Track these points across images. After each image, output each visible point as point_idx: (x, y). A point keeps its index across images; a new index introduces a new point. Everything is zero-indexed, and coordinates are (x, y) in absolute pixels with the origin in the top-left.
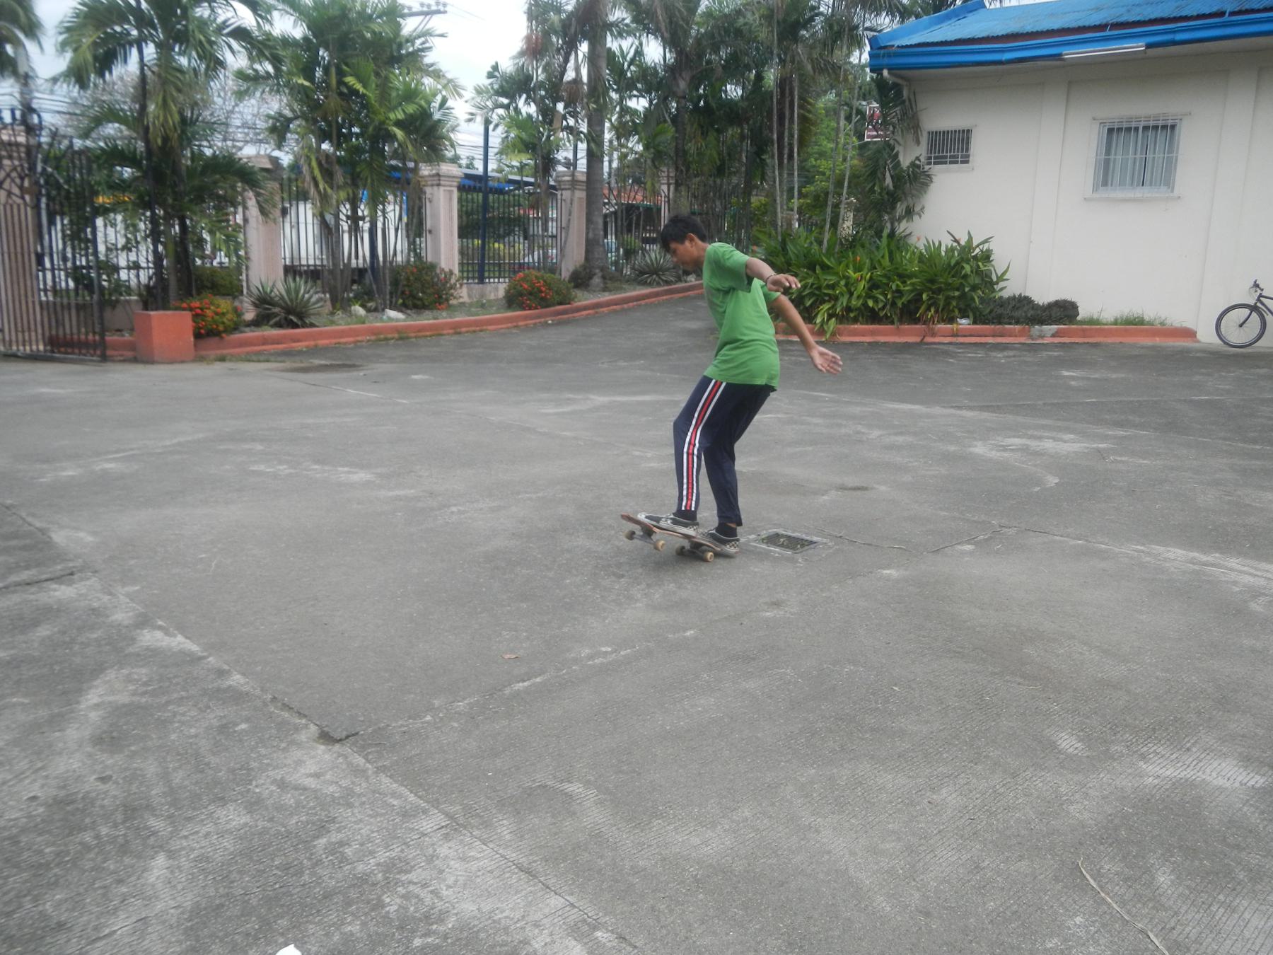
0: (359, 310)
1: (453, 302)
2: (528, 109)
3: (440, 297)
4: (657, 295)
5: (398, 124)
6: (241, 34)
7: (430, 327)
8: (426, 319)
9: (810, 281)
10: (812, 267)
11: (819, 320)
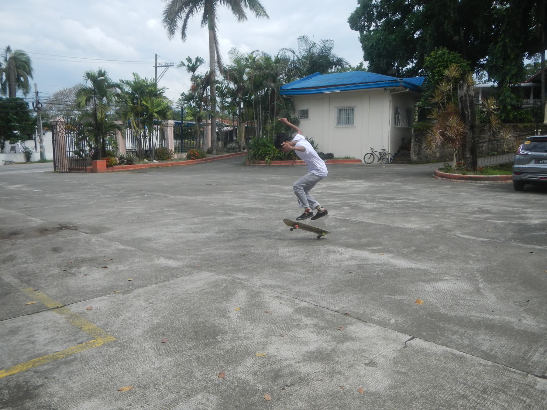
0: (147, 161)
1: (173, 158)
2: (193, 104)
4: (232, 155)
5: (156, 112)
6: (118, 95)
7: (165, 164)
8: (164, 163)
9: (264, 150)
10: (264, 146)
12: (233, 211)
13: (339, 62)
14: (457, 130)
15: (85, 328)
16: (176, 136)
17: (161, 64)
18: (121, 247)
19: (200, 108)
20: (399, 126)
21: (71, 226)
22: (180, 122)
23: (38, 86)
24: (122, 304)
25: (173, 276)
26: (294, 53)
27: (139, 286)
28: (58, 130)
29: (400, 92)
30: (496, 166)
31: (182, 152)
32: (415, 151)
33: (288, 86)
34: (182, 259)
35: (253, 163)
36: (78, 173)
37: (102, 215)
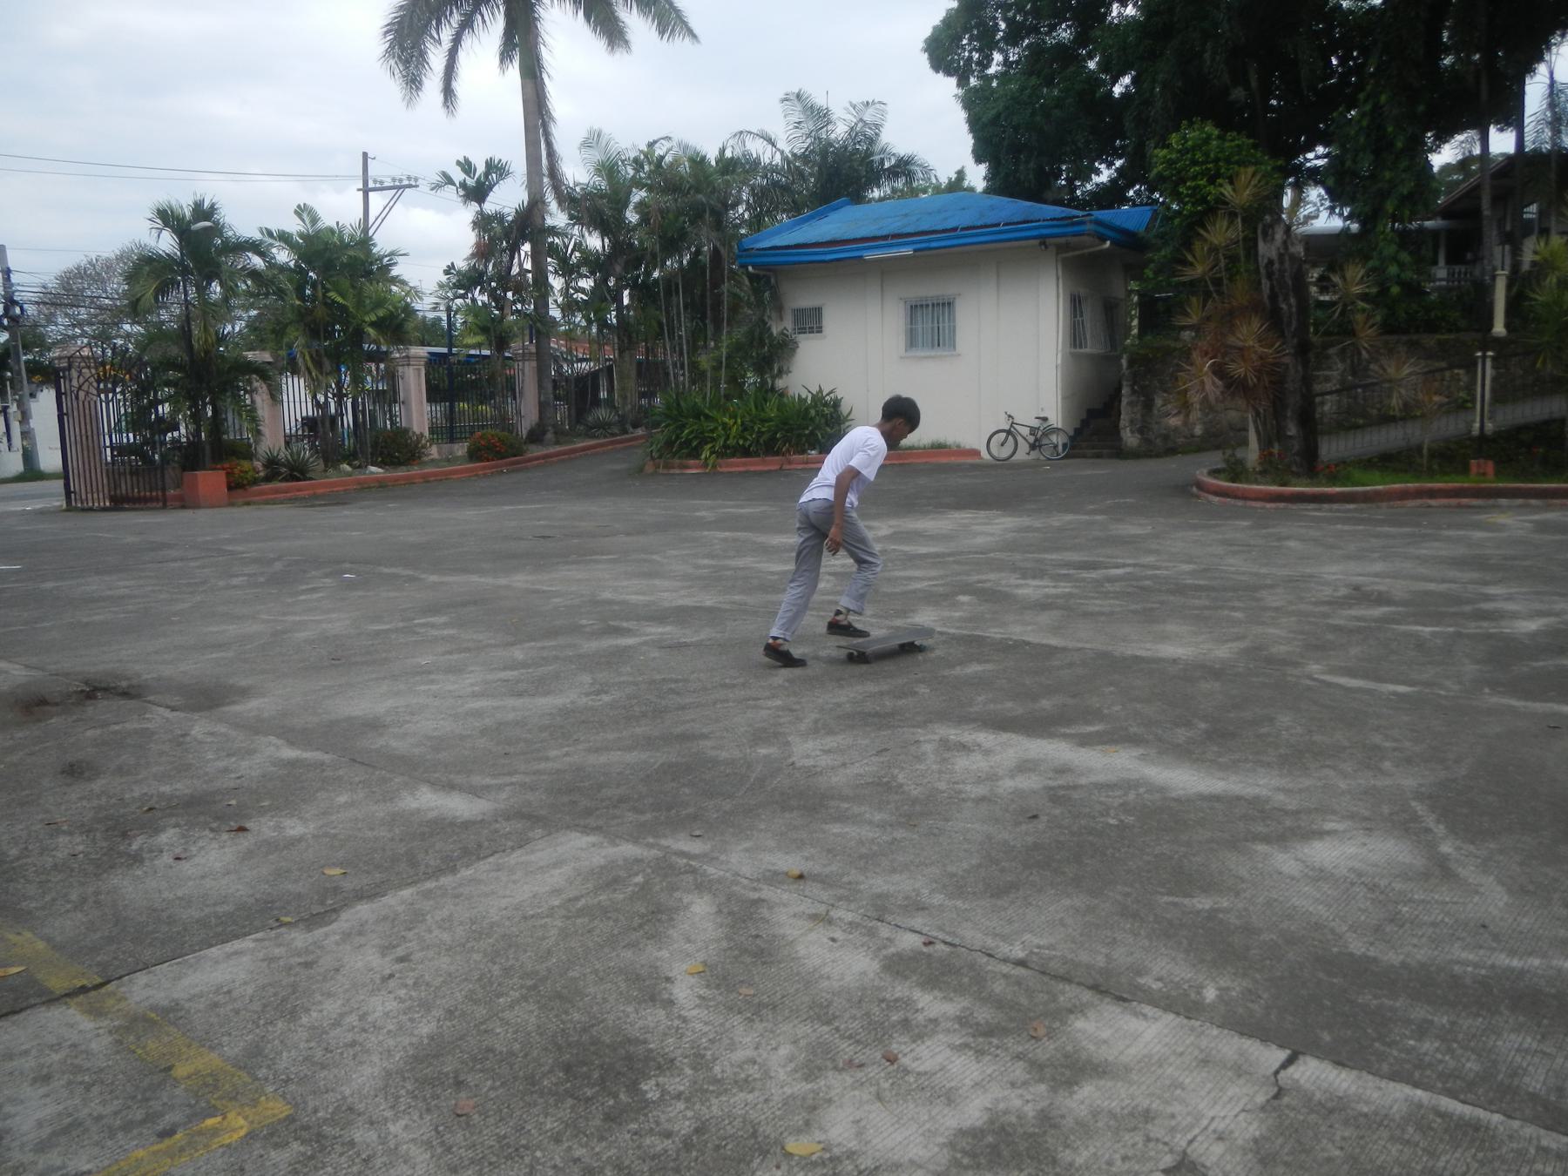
0: (346, 467)
1: (425, 459)
3: (413, 455)
4: (601, 445)
5: (372, 324)
6: (254, 274)
8: (401, 472)
9: (695, 427)
11: (703, 456)
12: (627, 620)
13: (904, 167)
14: (1261, 358)
15: (181, 1071)
16: (434, 394)
17: (381, 182)
18: (289, 753)
19: (501, 309)
20: (1082, 351)
21: (124, 684)
22: (445, 350)
23: (8, 251)
24: (308, 965)
25: (466, 852)
26: (773, 145)
27: (361, 896)
28: (75, 383)
29: (1086, 251)
30: (1369, 460)
31: (452, 440)
32: (1132, 422)
33: (757, 241)
34: (487, 788)
35: (667, 466)
36: (142, 509)
37: (220, 646)
